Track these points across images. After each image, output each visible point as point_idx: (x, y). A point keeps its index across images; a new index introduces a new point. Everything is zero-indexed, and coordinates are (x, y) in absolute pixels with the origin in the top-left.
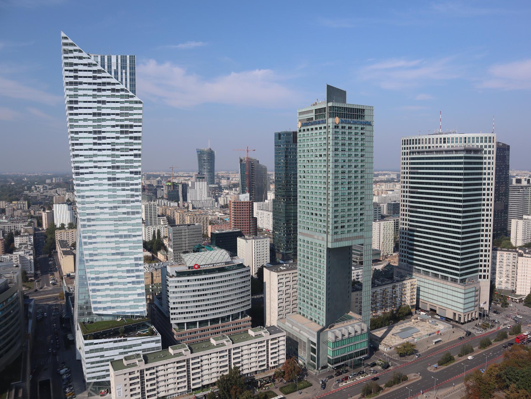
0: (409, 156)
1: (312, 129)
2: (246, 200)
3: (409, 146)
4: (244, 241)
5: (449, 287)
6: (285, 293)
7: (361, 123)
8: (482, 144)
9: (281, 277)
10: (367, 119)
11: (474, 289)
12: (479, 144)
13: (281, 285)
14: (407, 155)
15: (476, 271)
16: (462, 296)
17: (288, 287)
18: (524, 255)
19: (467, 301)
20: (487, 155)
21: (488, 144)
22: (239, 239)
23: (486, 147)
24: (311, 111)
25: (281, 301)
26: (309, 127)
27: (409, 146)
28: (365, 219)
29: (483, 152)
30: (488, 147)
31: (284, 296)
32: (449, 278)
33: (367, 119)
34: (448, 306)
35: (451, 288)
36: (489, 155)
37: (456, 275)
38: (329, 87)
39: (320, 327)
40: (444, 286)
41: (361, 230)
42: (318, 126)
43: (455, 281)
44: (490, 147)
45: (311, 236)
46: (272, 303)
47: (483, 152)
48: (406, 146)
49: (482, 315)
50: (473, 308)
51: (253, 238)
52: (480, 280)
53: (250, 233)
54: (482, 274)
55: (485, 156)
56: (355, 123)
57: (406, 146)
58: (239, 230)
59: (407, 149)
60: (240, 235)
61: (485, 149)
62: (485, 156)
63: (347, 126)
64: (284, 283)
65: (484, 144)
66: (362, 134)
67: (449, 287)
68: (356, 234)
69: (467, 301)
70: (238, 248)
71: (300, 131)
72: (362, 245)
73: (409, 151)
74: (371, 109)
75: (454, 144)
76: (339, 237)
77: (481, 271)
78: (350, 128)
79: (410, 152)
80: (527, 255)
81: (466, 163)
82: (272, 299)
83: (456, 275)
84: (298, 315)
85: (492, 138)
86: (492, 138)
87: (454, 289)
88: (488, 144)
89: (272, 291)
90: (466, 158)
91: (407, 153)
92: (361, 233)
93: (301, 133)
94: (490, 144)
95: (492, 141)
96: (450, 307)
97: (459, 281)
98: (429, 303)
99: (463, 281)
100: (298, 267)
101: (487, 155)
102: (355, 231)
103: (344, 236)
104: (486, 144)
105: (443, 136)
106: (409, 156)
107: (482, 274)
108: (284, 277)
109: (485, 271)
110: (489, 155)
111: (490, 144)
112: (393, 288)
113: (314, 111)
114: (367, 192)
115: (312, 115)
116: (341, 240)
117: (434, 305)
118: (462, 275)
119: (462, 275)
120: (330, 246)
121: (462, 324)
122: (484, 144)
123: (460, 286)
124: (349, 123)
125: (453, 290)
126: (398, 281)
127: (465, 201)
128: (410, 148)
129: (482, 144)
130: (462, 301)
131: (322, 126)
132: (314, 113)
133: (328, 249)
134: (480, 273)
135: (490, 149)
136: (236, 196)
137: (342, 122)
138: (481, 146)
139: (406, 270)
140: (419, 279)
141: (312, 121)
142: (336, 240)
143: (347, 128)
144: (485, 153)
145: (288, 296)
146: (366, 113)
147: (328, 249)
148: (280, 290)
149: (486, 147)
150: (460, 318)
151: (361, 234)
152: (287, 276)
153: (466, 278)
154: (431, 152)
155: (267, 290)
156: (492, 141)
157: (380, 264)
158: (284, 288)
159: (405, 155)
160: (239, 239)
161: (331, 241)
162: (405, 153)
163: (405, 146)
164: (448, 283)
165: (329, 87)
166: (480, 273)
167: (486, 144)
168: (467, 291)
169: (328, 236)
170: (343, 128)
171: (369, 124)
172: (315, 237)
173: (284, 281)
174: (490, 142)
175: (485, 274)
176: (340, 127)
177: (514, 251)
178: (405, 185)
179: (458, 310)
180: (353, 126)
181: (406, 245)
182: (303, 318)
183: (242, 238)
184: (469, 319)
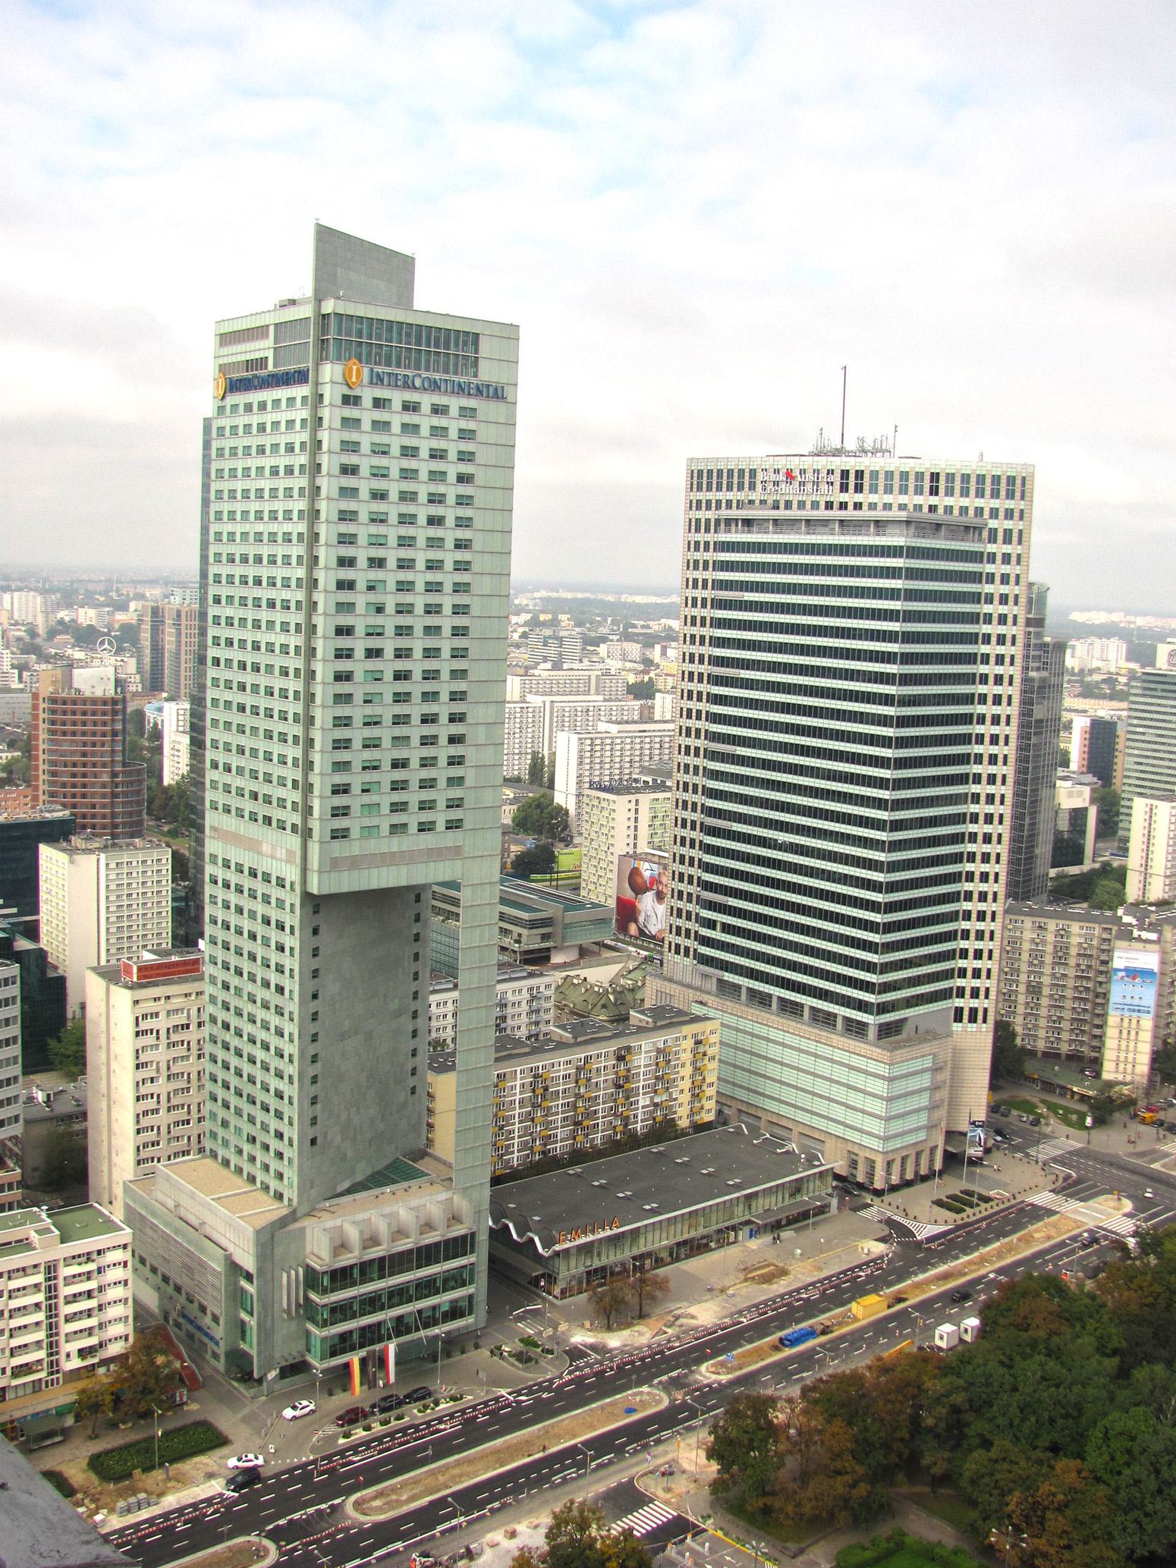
0: (711, 537)
1: (263, 406)
2: (99, 693)
3: (713, 496)
4: (63, 857)
5: (838, 1055)
6: (164, 1073)
7: (461, 390)
8: (980, 502)
9: (149, 1007)
10: (487, 373)
11: (928, 1062)
12: (971, 502)
13: (150, 1039)
14: (707, 530)
15: (945, 994)
16: (879, 1087)
17: (181, 1051)
18: (1136, 933)
19: (899, 1107)
20: (998, 548)
21: (1002, 504)
22: (45, 851)
23: (994, 513)
24: (260, 332)
25: (151, 1104)
26: (255, 397)
27: (713, 496)
28: (469, 782)
29: (985, 534)
30: (1001, 514)
31: (162, 1086)
32: (839, 1021)
33: (487, 373)
34: (833, 1128)
35: (845, 1057)
36: (1007, 549)
37: (862, 1006)
38: (326, 236)
39: (280, 1210)
40: (827, 1051)
41: (453, 825)
42: (282, 393)
43: (856, 1029)
44: (1009, 514)
45: (253, 846)
46: (115, 1114)
47: (985, 534)
48: (703, 496)
49: (953, 1161)
50: (922, 1136)
51: (104, 848)
52: (957, 1027)
53: (115, 826)
54: (966, 1003)
55: (991, 548)
56: (434, 386)
57: (703, 496)
58: (65, 814)
59: (708, 507)
60: (57, 833)
61: (993, 524)
62: (991, 548)
63: (397, 397)
64: (163, 1034)
65: (987, 503)
66: (376, 424)
67: (838, 1055)
68: (427, 840)
69: (899, 1107)
70: (43, 886)
71: (221, 410)
72: (454, 885)
73: (711, 515)
74: (510, 334)
75: (956, 501)
76: (352, 848)
77: (961, 992)
78: (409, 407)
79: (718, 521)
80: (1145, 935)
81: (912, 574)
82: (114, 1096)
83: (862, 1006)
84: (209, 1162)
85: (1018, 482)
86: (1018, 482)
87: (856, 1061)
88: (1002, 504)
89: (114, 1065)
90: (913, 552)
91: (708, 521)
92: (395, 840)
93: (226, 422)
94: (1010, 504)
95: (1018, 494)
96: (839, 1130)
97: (872, 1033)
98: (764, 1116)
99: (887, 1031)
100: (208, 969)
101: (998, 548)
102: (425, 828)
103: (374, 846)
104: (995, 503)
105: (851, 464)
106: (711, 537)
107: (966, 1003)
108: (161, 1006)
109: (975, 993)
110: (1007, 549)
111: (1010, 504)
112: (621, 1058)
113: (272, 329)
114: (477, 671)
115: (263, 348)
116: (354, 863)
117: (784, 1123)
118: (883, 1008)
119: (883, 1008)
120: (314, 889)
121: (878, 1193)
122: (987, 503)
123: (877, 1052)
124: (408, 385)
125: (851, 1068)
126: (642, 1030)
127: (903, 722)
128: (719, 503)
129: (980, 502)
130: (879, 1107)
131: (300, 391)
132: (270, 342)
133: (307, 896)
134: (959, 1002)
135: (1008, 524)
136: (59, 672)
137: (377, 380)
138: (979, 511)
139: (689, 986)
140: (732, 1020)
141: (262, 373)
142: (334, 864)
143: (397, 405)
144: (993, 537)
145: (181, 1084)
146: (485, 348)
147: (314, 903)
148: (143, 1059)
149: (994, 513)
150: (871, 1175)
151: (452, 839)
152: (177, 1002)
153: (904, 1020)
154: (792, 524)
155: (95, 1056)
156: (1018, 494)
157: (608, 962)
158: (161, 1055)
159: (698, 530)
160: (45, 851)
161: (316, 868)
162: (698, 521)
163: (700, 496)
164: (836, 1039)
165: (326, 236)
166: (959, 1002)
167: (995, 503)
168: (898, 1071)
169: (310, 844)
170: (378, 403)
171: (497, 393)
172: (266, 848)
173: (162, 1023)
174: (1010, 495)
175: (974, 1003)
176: (367, 402)
177: (1107, 920)
178: (697, 649)
179: (867, 1141)
180: (427, 400)
181: (691, 889)
182: (225, 1172)
183: (64, 850)
184: (909, 1176)
